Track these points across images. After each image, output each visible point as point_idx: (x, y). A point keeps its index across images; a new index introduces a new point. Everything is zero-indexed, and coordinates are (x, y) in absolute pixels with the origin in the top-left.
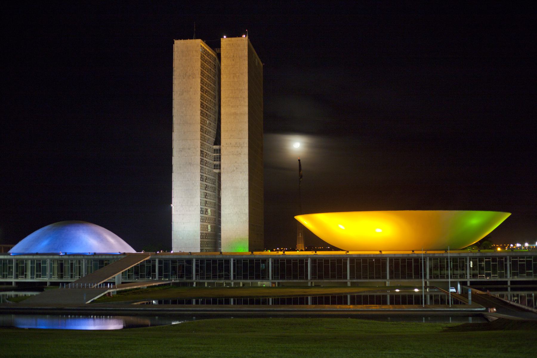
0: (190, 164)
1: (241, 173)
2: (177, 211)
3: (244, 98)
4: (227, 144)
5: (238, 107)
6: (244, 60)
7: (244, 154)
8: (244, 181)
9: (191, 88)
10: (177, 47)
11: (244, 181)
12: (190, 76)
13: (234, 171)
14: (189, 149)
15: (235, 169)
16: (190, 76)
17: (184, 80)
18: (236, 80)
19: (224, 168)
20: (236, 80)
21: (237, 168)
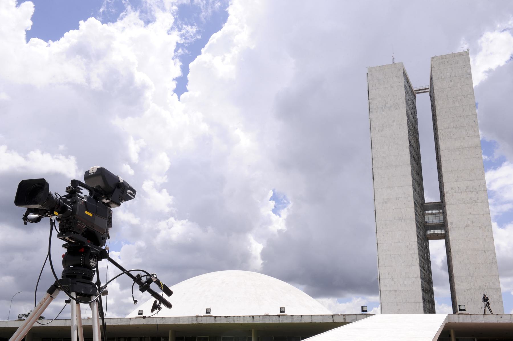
0: (400, 219)
2: (386, 286)
3: (472, 126)
5: (464, 138)
6: (467, 78)
7: (482, 202)
8: (487, 240)
9: (394, 121)
10: (371, 75)
12: (391, 107)
14: (397, 199)
15: (469, 223)
16: (391, 107)
17: (384, 113)
18: (457, 105)
19: (452, 223)
20: (457, 105)
21: (473, 222)
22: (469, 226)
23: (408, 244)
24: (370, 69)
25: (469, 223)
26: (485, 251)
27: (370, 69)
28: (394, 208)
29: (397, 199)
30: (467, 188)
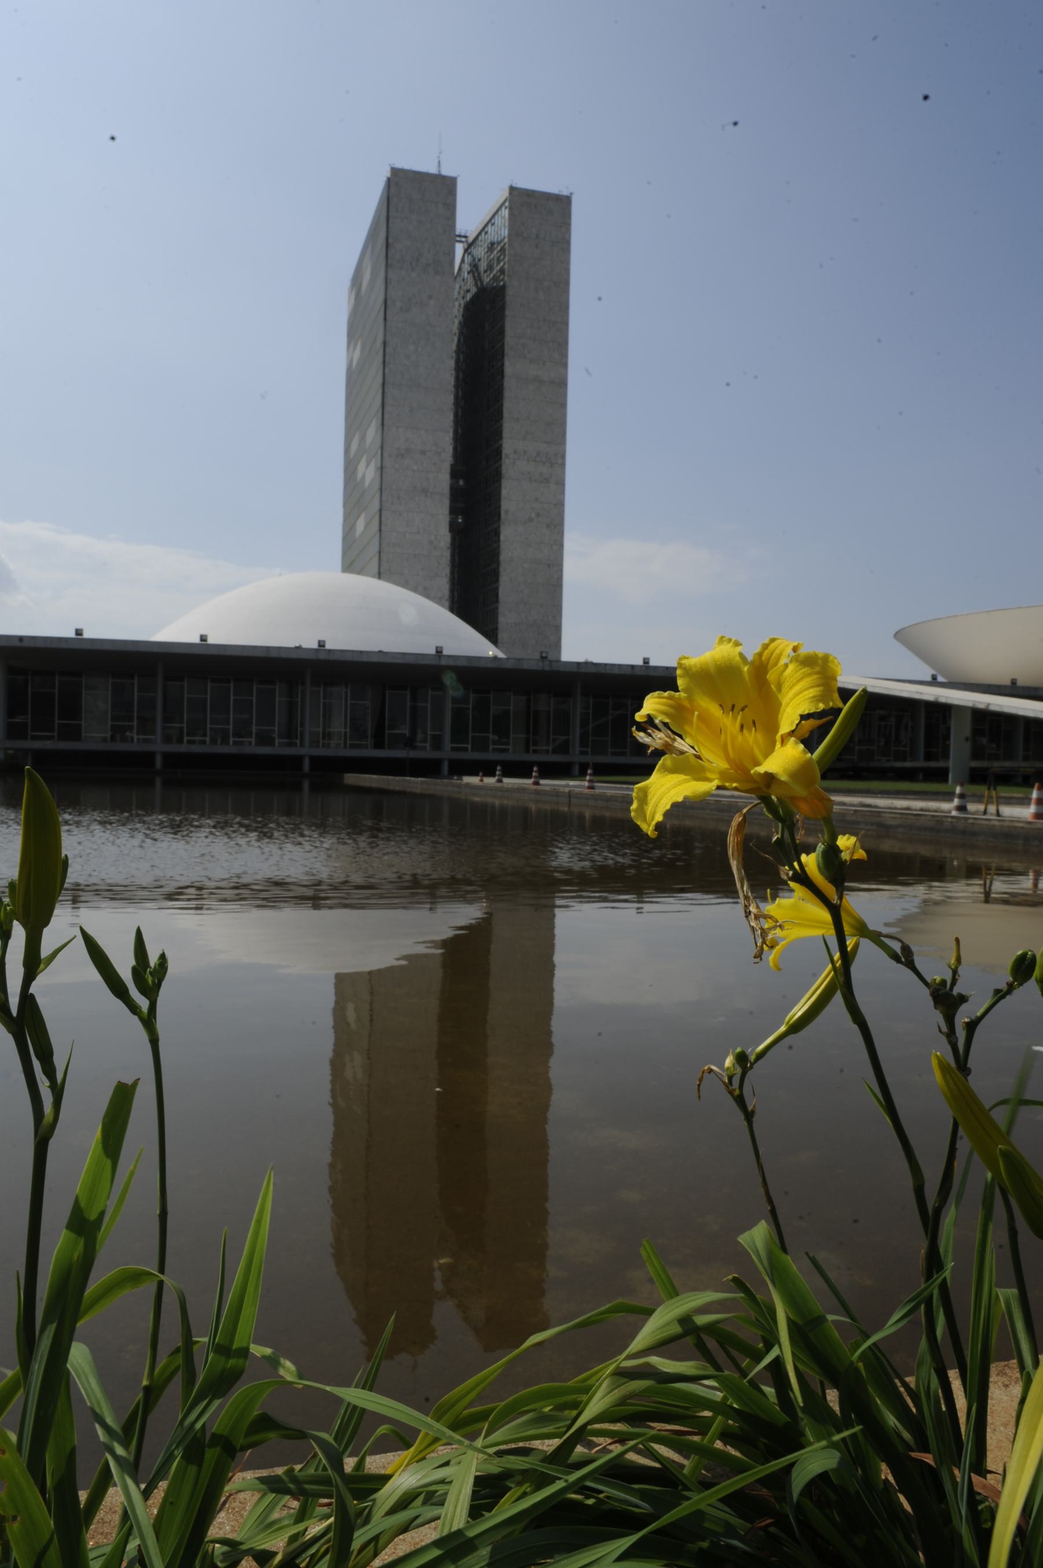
0: (425, 491)
1: (548, 526)
4: (515, 452)
8: (555, 547)
9: (430, 297)
11: (555, 547)
13: (531, 520)
14: (423, 453)
15: (533, 515)
19: (507, 512)
21: (538, 515)
22: (531, 520)
23: (433, 538)
24: (396, 172)
25: (533, 515)
26: (549, 566)
27: (396, 172)
28: (415, 468)
29: (423, 453)
30: (538, 454)
